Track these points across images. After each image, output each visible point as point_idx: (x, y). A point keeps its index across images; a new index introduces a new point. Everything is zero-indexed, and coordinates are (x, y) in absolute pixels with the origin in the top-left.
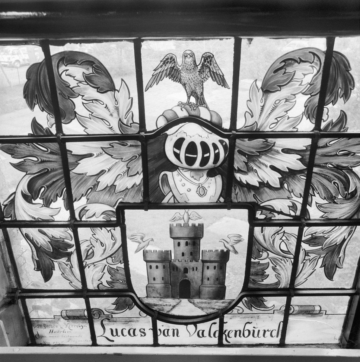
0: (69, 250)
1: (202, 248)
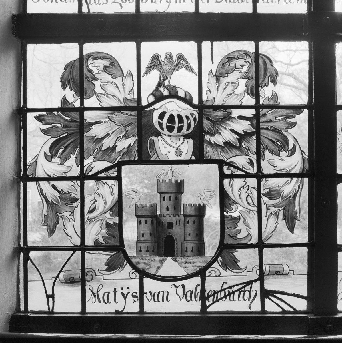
0: (75, 204)
1: (182, 203)
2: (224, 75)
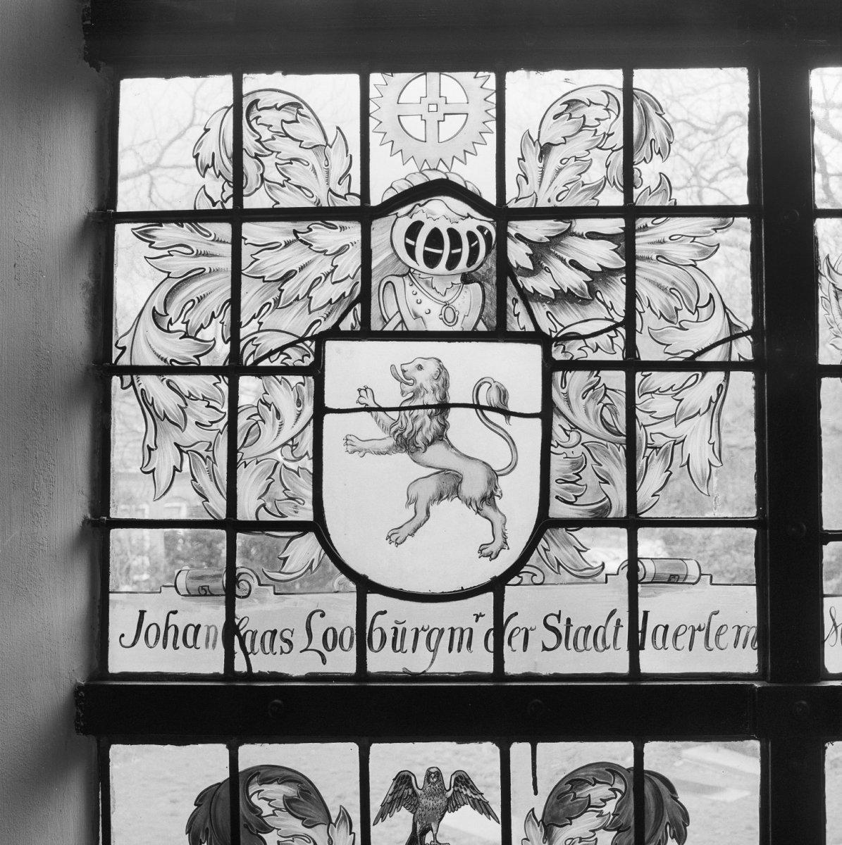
2: (562, 821)
